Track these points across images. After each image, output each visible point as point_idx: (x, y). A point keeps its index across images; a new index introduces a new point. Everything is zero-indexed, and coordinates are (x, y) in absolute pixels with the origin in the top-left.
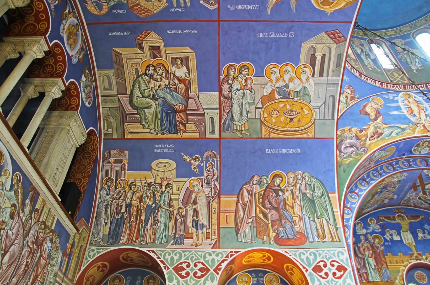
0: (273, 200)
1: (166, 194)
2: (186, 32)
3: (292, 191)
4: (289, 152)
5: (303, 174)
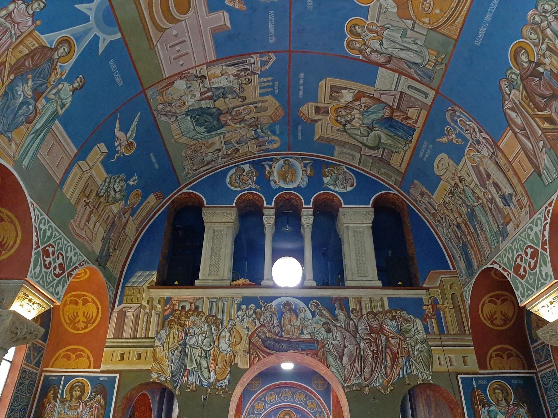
0: (542, 88)
1: (467, 189)
2: (301, 82)
3: (549, 49)
4: (493, 11)
5: (537, 9)
